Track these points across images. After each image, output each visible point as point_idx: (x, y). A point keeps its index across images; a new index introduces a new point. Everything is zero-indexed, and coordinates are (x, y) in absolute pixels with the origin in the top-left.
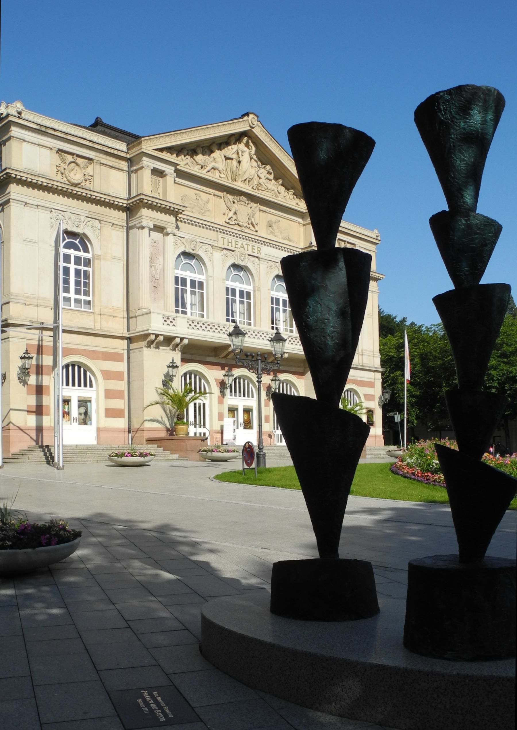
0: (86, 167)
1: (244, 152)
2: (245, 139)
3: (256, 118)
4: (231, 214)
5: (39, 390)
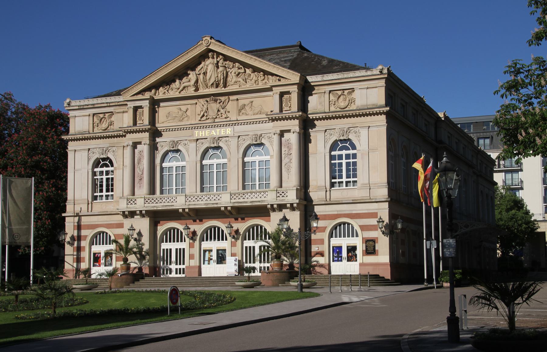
0: (110, 117)
1: (208, 64)
2: (210, 54)
3: (209, 38)
5: (79, 249)
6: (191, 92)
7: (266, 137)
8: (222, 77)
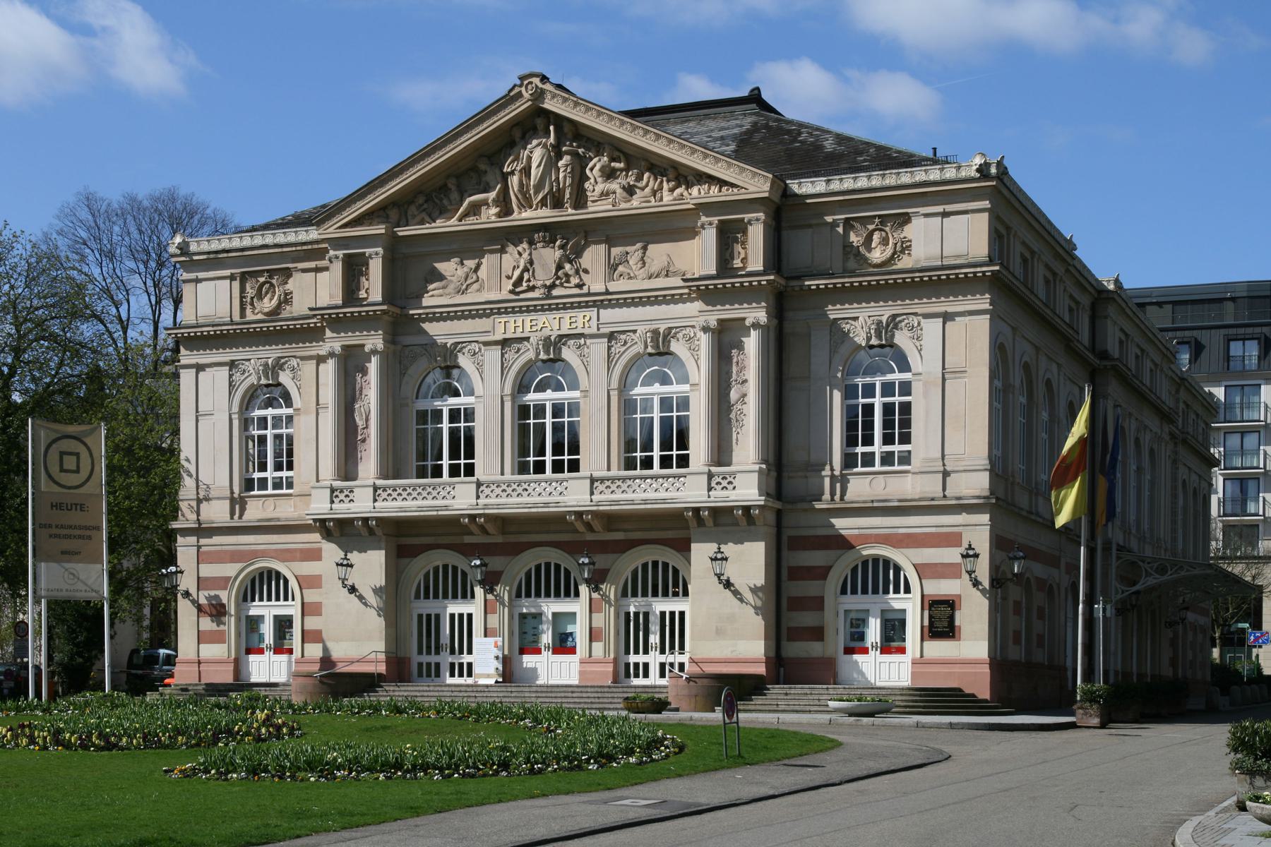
4: (517, 273)
6: (489, 217)
7: (680, 335)
8: (568, 181)
